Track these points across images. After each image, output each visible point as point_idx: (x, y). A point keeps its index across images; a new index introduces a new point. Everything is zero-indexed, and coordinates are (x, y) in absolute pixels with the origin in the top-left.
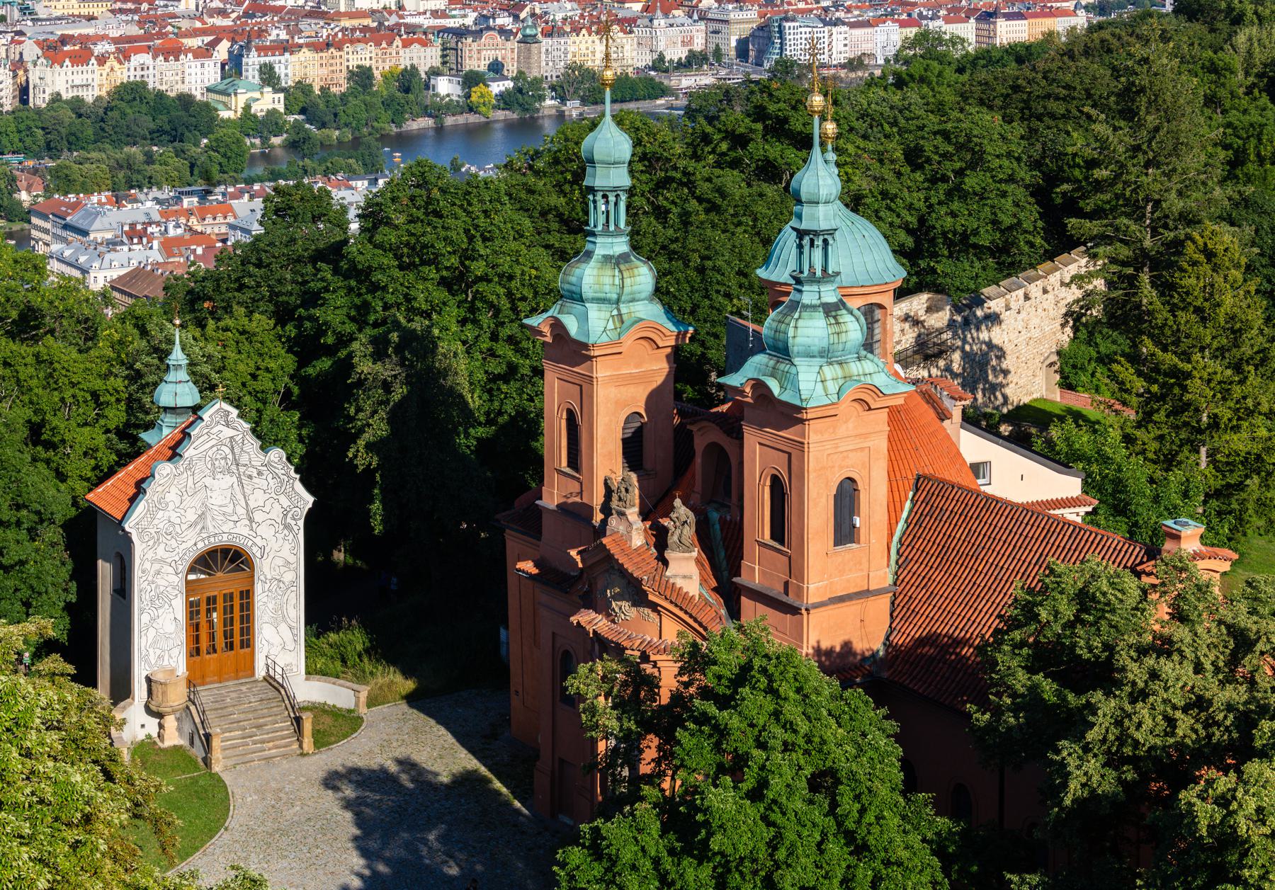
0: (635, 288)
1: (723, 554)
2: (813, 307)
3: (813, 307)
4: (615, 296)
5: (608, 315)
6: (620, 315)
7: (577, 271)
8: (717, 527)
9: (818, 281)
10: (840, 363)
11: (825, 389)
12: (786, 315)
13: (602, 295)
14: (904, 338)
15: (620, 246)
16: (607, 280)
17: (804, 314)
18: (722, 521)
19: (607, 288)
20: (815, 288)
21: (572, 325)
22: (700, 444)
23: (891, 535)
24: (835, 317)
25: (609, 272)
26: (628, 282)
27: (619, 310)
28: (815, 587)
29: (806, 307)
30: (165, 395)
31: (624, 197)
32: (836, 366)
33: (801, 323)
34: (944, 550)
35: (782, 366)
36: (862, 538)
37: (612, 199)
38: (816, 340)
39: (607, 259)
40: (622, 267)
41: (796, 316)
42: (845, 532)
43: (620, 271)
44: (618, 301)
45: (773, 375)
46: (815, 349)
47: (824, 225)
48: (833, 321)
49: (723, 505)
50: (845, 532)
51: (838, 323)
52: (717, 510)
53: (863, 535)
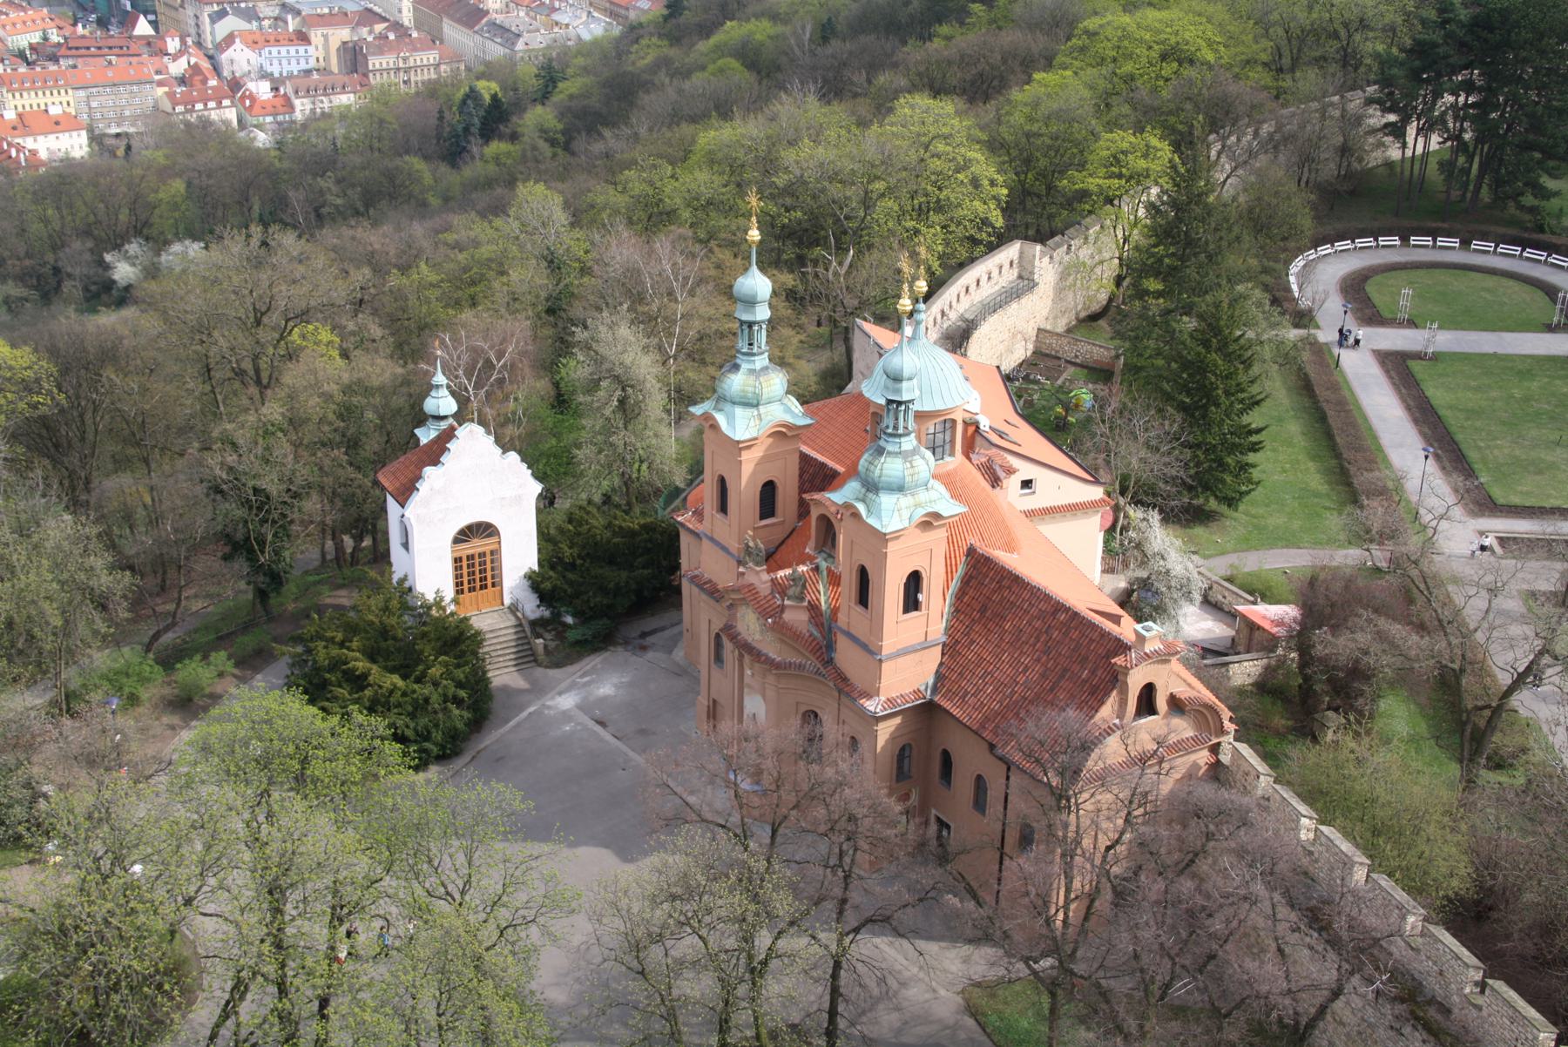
6: (759, 415)
7: (728, 381)
9: (900, 436)
11: (900, 516)
12: (875, 458)
15: (762, 361)
17: (889, 459)
18: (829, 570)
21: (721, 419)
28: (889, 644)
29: (889, 453)
31: (764, 326)
32: (910, 497)
34: (983, 610)
35: (870, 495)
36: (923, 606)
37: (756, 328)
39: (752, 372)
41: (882, 460)
42: (911, 603)
45: (863, 501)
47: (905, 398)
48: (908, 465)
49: (831, 556)
50: (911, 603)
52: (825, 560)
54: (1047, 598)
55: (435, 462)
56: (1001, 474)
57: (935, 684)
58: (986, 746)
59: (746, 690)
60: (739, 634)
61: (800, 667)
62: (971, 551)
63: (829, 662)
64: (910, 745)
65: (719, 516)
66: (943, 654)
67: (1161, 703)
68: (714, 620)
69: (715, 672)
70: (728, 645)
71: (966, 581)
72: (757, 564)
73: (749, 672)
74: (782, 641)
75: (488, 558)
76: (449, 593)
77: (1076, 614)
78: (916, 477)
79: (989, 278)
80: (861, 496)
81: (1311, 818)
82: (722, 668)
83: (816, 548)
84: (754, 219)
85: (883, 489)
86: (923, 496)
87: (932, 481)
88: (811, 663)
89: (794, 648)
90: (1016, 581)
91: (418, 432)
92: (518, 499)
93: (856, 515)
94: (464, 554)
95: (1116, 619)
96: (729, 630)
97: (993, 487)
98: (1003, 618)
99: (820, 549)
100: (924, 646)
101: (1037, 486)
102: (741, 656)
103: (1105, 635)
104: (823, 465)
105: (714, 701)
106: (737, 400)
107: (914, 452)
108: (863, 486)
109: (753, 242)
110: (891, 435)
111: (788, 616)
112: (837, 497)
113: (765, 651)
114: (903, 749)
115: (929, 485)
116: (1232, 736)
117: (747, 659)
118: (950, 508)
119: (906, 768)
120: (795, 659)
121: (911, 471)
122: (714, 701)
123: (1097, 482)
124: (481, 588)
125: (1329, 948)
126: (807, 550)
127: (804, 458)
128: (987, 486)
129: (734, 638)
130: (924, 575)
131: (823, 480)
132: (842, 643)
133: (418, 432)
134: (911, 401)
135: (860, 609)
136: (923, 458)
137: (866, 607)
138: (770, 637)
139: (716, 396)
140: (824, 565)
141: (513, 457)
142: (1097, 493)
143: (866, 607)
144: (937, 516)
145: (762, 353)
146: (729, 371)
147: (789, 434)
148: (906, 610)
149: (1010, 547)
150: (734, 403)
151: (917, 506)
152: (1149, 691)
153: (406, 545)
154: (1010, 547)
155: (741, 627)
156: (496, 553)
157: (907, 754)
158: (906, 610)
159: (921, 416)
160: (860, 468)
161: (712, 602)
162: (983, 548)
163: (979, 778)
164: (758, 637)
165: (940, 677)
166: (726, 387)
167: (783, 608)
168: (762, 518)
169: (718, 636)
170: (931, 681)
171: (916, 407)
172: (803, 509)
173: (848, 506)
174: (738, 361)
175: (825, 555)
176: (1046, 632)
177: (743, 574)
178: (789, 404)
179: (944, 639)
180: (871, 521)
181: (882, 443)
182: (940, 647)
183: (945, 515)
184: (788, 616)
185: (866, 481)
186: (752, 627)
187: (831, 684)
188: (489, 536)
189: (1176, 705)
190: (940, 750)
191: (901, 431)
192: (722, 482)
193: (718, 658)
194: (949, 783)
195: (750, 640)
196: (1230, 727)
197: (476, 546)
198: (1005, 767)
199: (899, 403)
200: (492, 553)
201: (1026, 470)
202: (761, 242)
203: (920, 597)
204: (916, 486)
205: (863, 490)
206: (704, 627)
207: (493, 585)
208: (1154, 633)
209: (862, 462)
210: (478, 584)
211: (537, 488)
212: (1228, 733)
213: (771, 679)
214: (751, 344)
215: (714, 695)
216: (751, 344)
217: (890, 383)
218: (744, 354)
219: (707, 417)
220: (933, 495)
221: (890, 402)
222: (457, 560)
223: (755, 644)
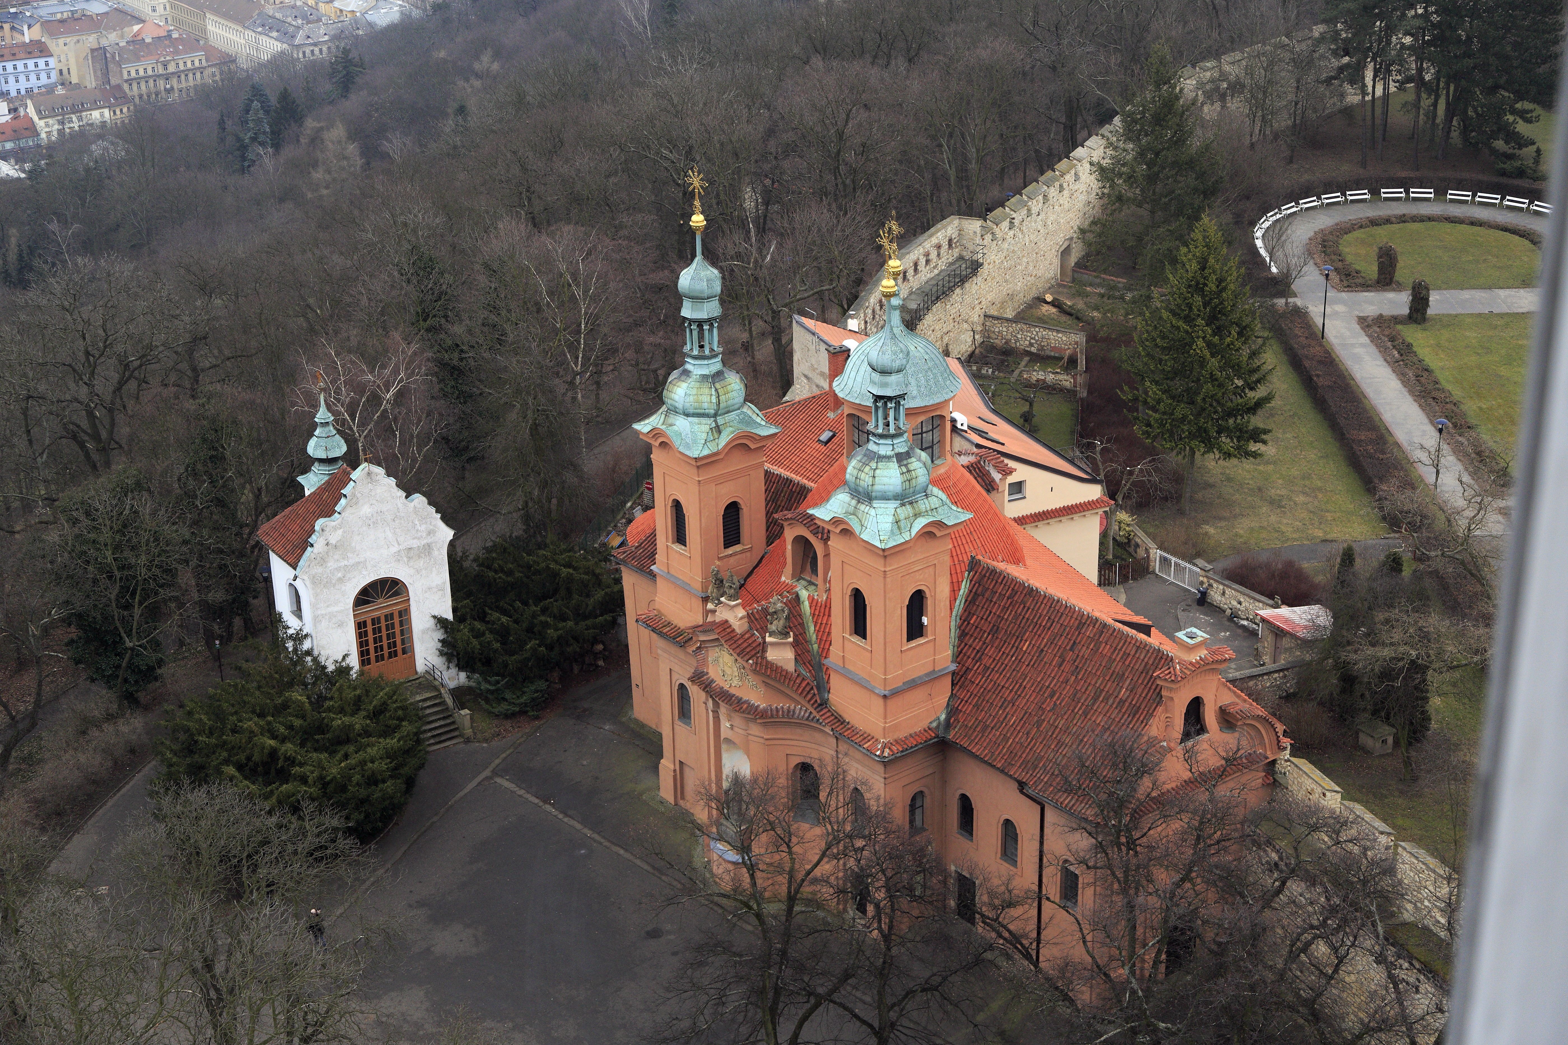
0: (730, 402)
1: (812, 628)
2: (888, 458)
3: (888, 458)
4: (712, 412)
5: (708, 427)
6: (717, 426)
8: (807, 603)
9: (893, 437)
10: (911, 503)
13: (702, 411)
14: (940, 263)
15: (715, 365)
16: (705, 398)
17: (880, 464)
18: (811, 599)
19: (706, 405)
20: (889, 442)
22: (790, 534)
23: (951, 609)
24: (906, 465)
25: (706, 391)
26: (722, 398)
27: (716, 421)
30: (314, 448)
31: (716, 325)
33: (878, 472)
35: (862, 507)
37: (706, 327)
38: (891, 488)
39: (704, 377)
40: (718, 385)
42: (915, 630)
43: (716, 390)
44: (715, 415)
46: (890, 494)
48: (905, 470)
49: (811, 583)
50: (915, 630)
51: (909, 471)
52: (806, 588)
53: (930, 630)
54: (1069, 610)
55: (329, 512)
56: (997, 476)
57: (948, 720)
58: (1015, 785)
59: (724, 747)
60: (712, 681)
61: (789, 713)
62: (974, 564)
63: (823, 704)
64: (921, 792)
65: (677, 547)
66: (953, 684)
67: (1210, 717)
68: (676, 668)
69: (680, 727)
70: (696, 693)
71: (972, 600)
72: (731, 598)
73: (725, 724)
74: (766, 684)
75: (396, 620)
76: (354, 661)
77: (1105, 625)
78: (914, 482)
79: (928, 262)
80: (851, 509)
81: (1389, 834)
82: (688, 723)
83: (793, 577)
84: (697, 203)
85: (877, 498)
86: (923, 505)
87: (930, 487)
88: (802, 708)
89: (782, 692)
90: (1032, 592)
91: (301, 479)
92: (427, 549)
93: (847, 532)
94: (368, 618)
95: (1145, 629)
96: (698, 677)
97: (988, 491)
98: (1020, 638)
99: (798, 576)
100: (932, 678)
101: (1028, 489)
102: (716, 705)
103: (1141, 647)
104: (788, 481)
105: (681, 763)
106: (691, 411)
107: (908, 455)
108: (853, 497)
109: (698, 228)
110: (881, 436)
111: (772, 655)
112: (823, 513)
113: (745, 698)
114: (914, 799)
115: (929, 492)
116: (1288, 752)
117: (723, 710)
118: (955, 516)
119: (918, 823)
120: (783, 704)
121: (908, 476)
122: (681, 763)
123: (1093, 481)
124: (390, 657)
125: (1422, 977)
126: (783, 579)
127: (767, 474)
128: (984, 493)
129: (707, 687)
130: (928, 594)
131: (789, 499)
132: (836, 682)
133: (301, 479)
134: (902, 396)
135: (856, 639)
136: (919, 460)
137: (864, 637)
138: (752, 680)
139: (664, 408)
140: (804, 594)
141: (419, 500)
142: (1094, 492)
143: (864, 637)
144: (940, 524)
145: (715, 356)
146: (679, 378)
147: (753, 446)
148: (911, 637)
149: (1017, 558)
150: (687, 415)
151: (917, 515)
152: (1195, 707)
153: (298, 612)
154: (1017, 558)
155: (712, 673)
156: (405, 613)
157: (918, 804)
158: (911, 637)
159: (911, 413)
160: (848, 476)
161: (674, 649)
162: (986, 560)
163: (1008, 823)
164: (735, 682)
165: (952, 711)
166: (673, 396)
167: (764, 646)
168: (727, 546)
169: (682, 686)
170: (943, 717)
171: (909, 403)
172: (774, 532)
173: (836, 521)
174: (688, 367)
175: (803, 583)
176: (1071, 649)
177: (713, 612)
178: (749, 413)
179: (953, 667)
180: (864, 536)
181: (871, 446)
182: (948, 681)
183: (949, 523)
184: (772, 655)
185: (857, 491)
186: (728, 671)
187: (828, 730)
188: (396, 594)
189: (1227, 719)
190: (957, 796)
191: (892, 430)
192: (677, 506)
193: (684, 711)
194: (971, 834)
195: (726, 687)
196: (1287, 742)
197: (380, 607)
198: (1038, 808)
199: (890, 399)
200: (400, 614)
201: (1021, 472)
202: (706, 227)
203: (925, 620)
204: (914, 493)
205: (854, 502)
206: (665, 677)
207: (404, 652)
208: (1199, 639)
209: (850, 469)
210: (386, 651)
211: (448, 534)
212: (1285, 749)
213: (755, 730)
214: (701, 347)
215: (680, 756)
216: (701, 347)
217: (876, 376)
218: (695, 358)
219: (656, 433)
220: (934, 502)
221: (877, 398)
222: (360, 626)
223: (733, 691)
